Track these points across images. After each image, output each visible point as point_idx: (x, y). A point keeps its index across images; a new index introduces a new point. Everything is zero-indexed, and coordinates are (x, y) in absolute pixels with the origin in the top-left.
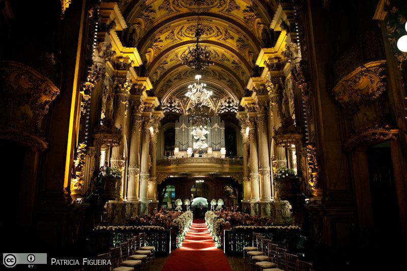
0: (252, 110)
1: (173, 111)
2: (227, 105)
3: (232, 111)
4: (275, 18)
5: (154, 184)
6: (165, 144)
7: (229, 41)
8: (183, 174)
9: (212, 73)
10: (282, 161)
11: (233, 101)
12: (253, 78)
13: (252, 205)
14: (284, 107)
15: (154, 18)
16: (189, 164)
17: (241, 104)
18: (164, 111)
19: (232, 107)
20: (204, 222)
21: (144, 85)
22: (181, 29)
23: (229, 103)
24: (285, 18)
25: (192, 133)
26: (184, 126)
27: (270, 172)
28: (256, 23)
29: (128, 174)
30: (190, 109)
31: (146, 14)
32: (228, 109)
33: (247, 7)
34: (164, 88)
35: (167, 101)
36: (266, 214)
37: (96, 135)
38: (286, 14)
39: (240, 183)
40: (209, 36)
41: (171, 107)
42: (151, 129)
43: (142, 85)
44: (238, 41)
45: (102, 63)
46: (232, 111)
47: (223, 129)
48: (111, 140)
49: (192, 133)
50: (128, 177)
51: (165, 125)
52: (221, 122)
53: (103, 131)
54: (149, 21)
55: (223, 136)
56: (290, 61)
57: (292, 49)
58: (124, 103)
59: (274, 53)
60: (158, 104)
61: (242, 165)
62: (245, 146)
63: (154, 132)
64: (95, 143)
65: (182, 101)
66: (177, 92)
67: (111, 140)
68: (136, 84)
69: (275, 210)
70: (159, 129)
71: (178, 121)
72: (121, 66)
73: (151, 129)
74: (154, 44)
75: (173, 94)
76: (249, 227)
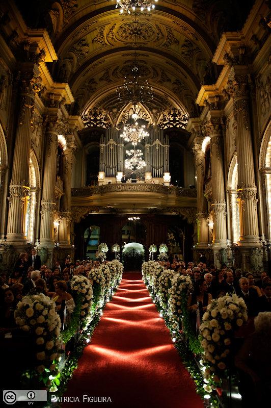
1: (98, 126)
9: (152, 71)
11: (180, 113)
19: (178, 121)
23: (174, 115)
26: (112, 142)
32: (172, 124)
35: (90, 113)
41: (95, 120)
46: (178, 126)
47: (167, 146)
51: (87, 145)
52: (164, 137)
55: (167, 157)
61: (195, 196)
62: (199, 168)
71: (105, 136)
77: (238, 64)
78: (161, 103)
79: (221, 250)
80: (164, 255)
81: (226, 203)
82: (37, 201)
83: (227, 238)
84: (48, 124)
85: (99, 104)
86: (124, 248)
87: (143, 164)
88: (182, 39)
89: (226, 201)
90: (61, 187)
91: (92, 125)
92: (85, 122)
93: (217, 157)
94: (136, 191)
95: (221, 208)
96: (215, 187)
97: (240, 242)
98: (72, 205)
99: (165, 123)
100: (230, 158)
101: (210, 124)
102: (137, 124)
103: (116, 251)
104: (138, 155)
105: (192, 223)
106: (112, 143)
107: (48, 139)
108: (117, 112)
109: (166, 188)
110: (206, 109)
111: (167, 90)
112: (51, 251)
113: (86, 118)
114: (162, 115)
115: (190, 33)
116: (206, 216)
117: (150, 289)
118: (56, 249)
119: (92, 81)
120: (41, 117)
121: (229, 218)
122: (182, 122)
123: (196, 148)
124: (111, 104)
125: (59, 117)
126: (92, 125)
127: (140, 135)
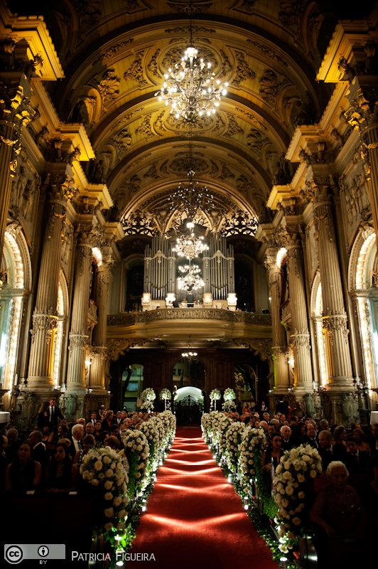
1: (142, 233)
3: (245, 233)
9: (211, 165)
11: (247, 217)
19: (244, 226)
20: (199, 434)
23: (240, 219)
26: (160, 254)
30: (172, 229)
32: (238, 231)
35: (132, 217)
41: (138, 226)
46: (245, 233)
47: (231, 259)
52: (228, 247)
55: (232, 273)
62: (274, 288)
65: (158, 217)
66: (149, 201)
71: (150, 247)
77: (317, 163)
78: (222, 203)
79: (306, 396)
80: (231, 403)
81: (310, 334)
82: (64, 333)
83: (313, 380)
84: (80, 235)
85: (143, 205)
86: (175, 394)
87: (201, 284)
88: (248, 128)
89: (309, 331)
90: (95, 314)
91: (134, 233)
92: (125, 228)
93: (296, 274)
94: (190, 318)
95: (303, 340)
96: (294, 313)
97: (329, 385)
98: (109, 337)
99: (228, 228)
100: (313, 275)
101: (286, 233)
102: (193, 235)
103: (166, 399)
104: (195, 272)
105: (267, 360)
106: (160, 256)
107: (79, 253)
108: (166, 216)
109: (230, 313)
110: (280, 213)
111: (230, 188)
112: (81, 400)
113: (126, 223)
114: (224, 219)
115: (257, 121)
116: (285, 351)
117: (214, 450)
118: (88, 397)
119: (135, 178)
120: (71, 226)
121: (314, 352)
122: (250, 227)
123: (269, 262)
124: (158, 206)
125: (95, 226)
126: (134, 233)
127: (197, 249)
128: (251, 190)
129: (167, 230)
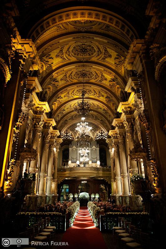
0: (116, 138)
1: (68, 138)
2: (101, 135)
3: (103, 138)
4: (127, 85)
5: (56, 183)
6: (63, 158)
7: (101, 98)
8: (74, 177)
10: (135, 169)
11: (104, 132)
12: (116, 119)
13: (117, 198)
14: (135, 136)
15: (58, 85)
16: (77, 171)
17: (109, 134)
18: (63, 138)
21: (51, 123)
22: (73, 91)
23: (102, 133)
24: (133, 85)
25: (79, 152)
26: (74, 147)
27: (128, 176)
28: (116, 88)
29: (39, 178)
31: (53, 83)
32: (101, 137)
33: (111, 79)
34: (63, 125)
35: (65, 133)
36: (126, 204)
37: (21, 153)
38: (134, 83)
39: (109, 183)
40: (89, 95)
41: (67, 136)
42: (55, 149)
43: (50, 123)
44: (106, 98)
45: (27, 111)
46: (103, 138)
47: (98, 149)
48: (30, 157)
49: (79, 152)
50: (39, 180)
52: (97, 145)
53: (25, 151)
54: (55, 87)
55: (98, 154)
56: (137, 109)
57: (138, 103)
58: (39, 134)
59: (127, 105)
60: (59, 134)
61: (110, 171)
62: (112, 159)
63: (56, 151)
64: (20, 158)
67: (30, 157)
68: (46, 123)
69: (132, 201)
70: (60, 149)
71: (71, 145)
72: (38, 112)
73: (55, 149)
74: (58, 100)
75: (68, 128)
76: (116, 213)
128: (105, 125)
129: (77, 137)
